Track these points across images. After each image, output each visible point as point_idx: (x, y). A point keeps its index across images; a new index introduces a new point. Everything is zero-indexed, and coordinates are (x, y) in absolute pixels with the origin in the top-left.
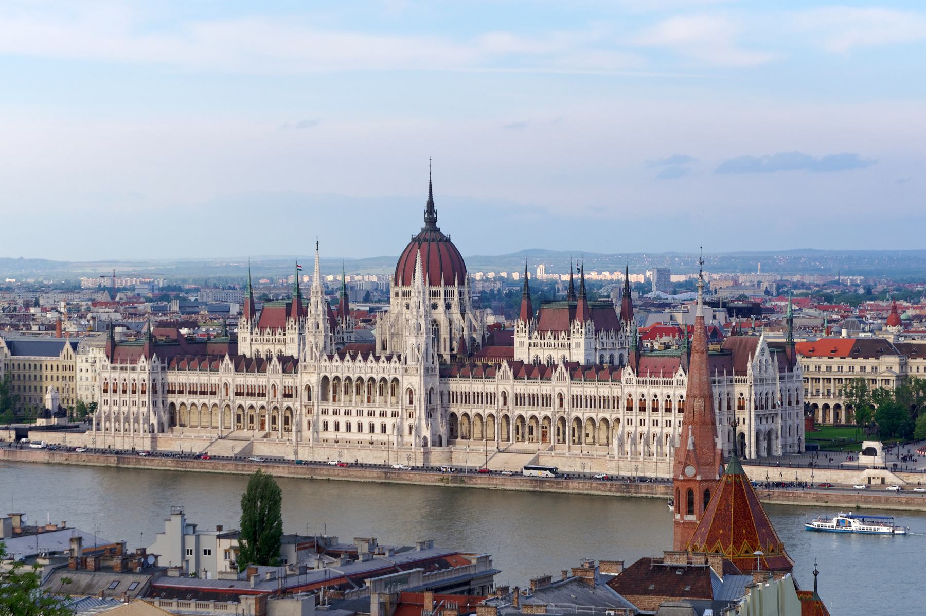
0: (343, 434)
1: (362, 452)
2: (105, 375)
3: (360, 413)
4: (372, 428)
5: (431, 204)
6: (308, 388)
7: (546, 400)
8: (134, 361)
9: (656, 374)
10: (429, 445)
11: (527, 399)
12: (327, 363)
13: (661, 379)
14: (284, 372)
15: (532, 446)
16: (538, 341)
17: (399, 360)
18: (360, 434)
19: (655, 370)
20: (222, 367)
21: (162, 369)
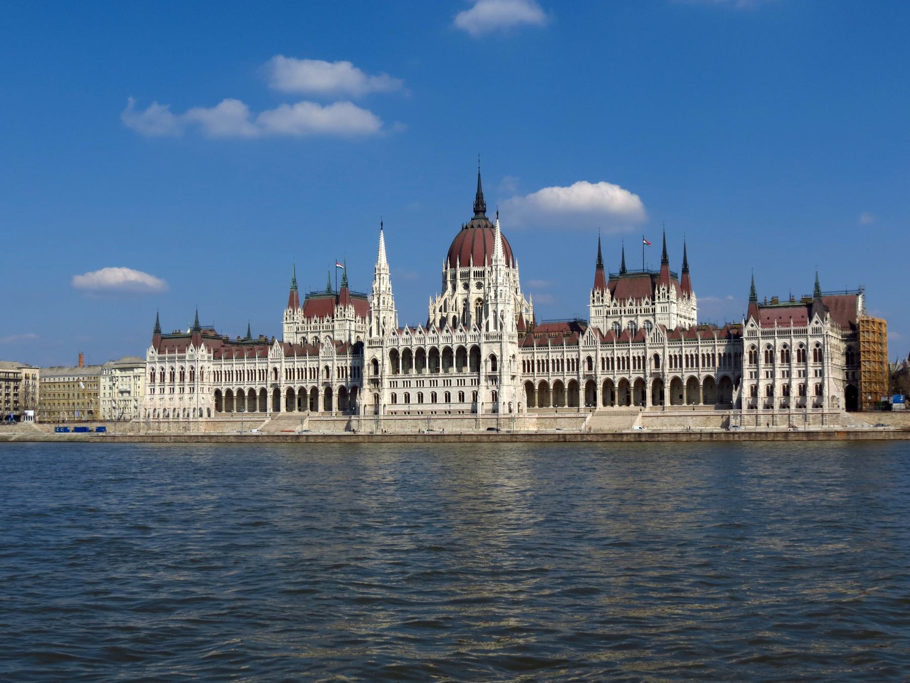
0: (414, 406)
1: (439, 421)
3: (434, 383)
4: (448, 397)
5: (479, 197)
6: (375, 362)
8: (184, 351)
9: (788, 324)
11: (616, 363)
12: (395, 337)
13: (792, 328)
14: (338, 354)
15: (624, 408)
17: (480, 328)
19: (780, 321)
21: (209, 358)
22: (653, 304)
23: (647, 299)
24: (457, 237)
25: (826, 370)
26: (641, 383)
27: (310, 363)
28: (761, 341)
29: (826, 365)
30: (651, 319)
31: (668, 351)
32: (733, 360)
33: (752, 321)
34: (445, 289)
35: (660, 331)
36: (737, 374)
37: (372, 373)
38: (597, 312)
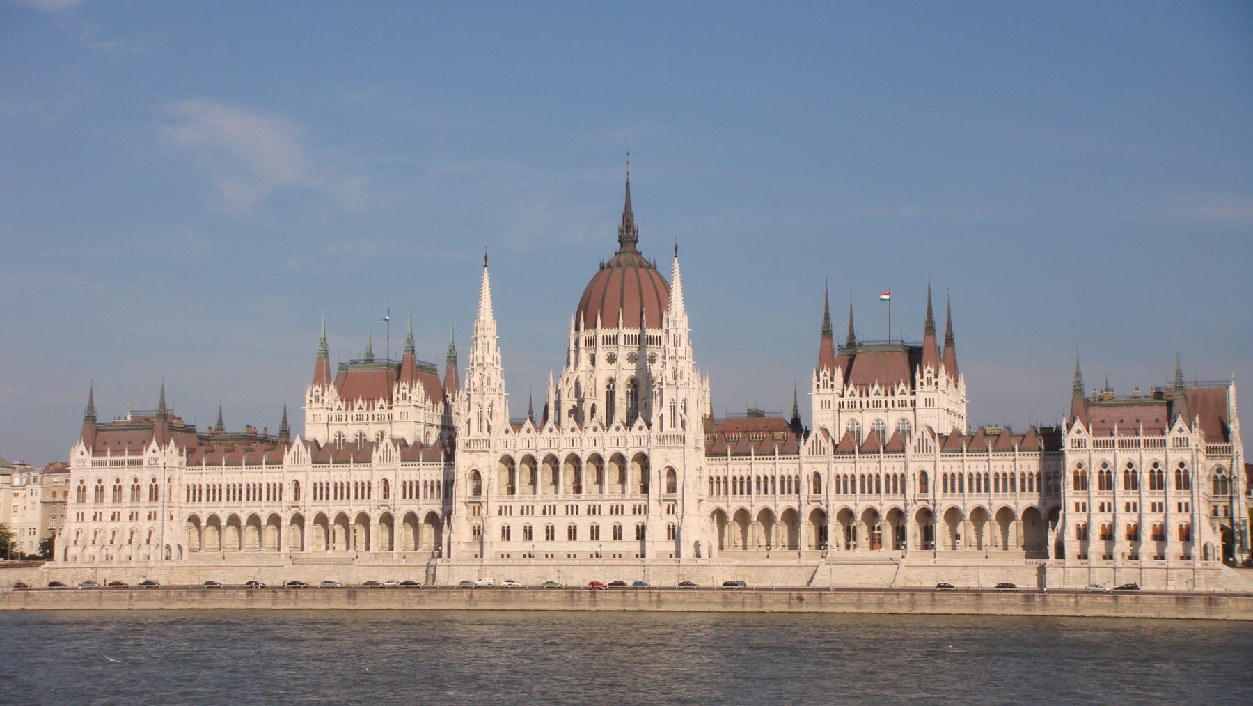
2: (83, 474)
4: (595, 534)
5: (628, 218)
6: (477, 475)
7: (898, 483)
8: (139, 451)
10: (704, 553)
11: (858, 483)
13: (1142, 438)
14: (404, 460)
16: (857, 399)
17: (649, 425)
18: (573, 543)
19: (1124, 425)
20: (287, 458)
21: (181, 463)
22: (914, 394)
23: (902, 386)
24: (595, 280)
25: (1196, 503)
26: (897, 516)
27: (353, 474)
28: (1094, 456)
29: (1195, 494)
30: (909, 415)
31: (942, 465)
32: (1049, 482)
33: (1078, 425)
34: (568, 363)
35: (927, 435)
36: (1051, 503)
37: (470, 493)
38: (826, 404)
